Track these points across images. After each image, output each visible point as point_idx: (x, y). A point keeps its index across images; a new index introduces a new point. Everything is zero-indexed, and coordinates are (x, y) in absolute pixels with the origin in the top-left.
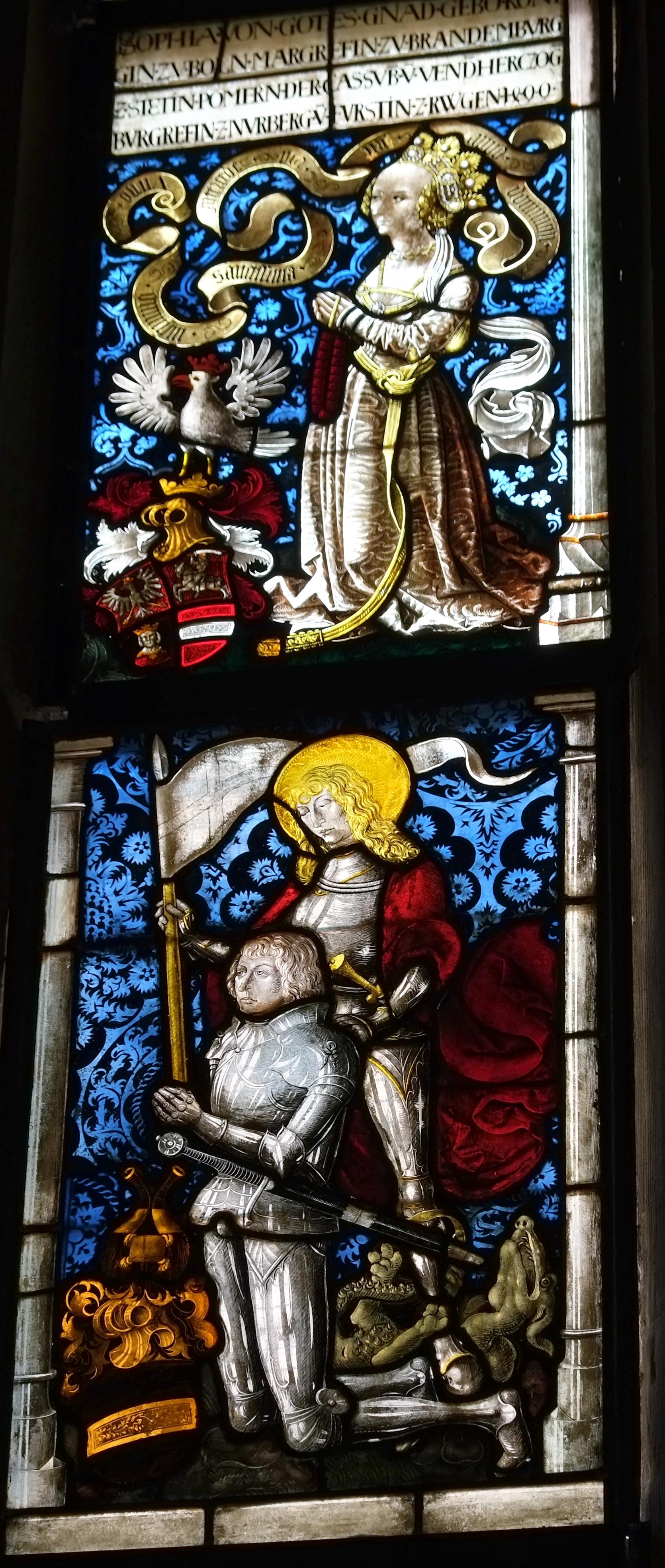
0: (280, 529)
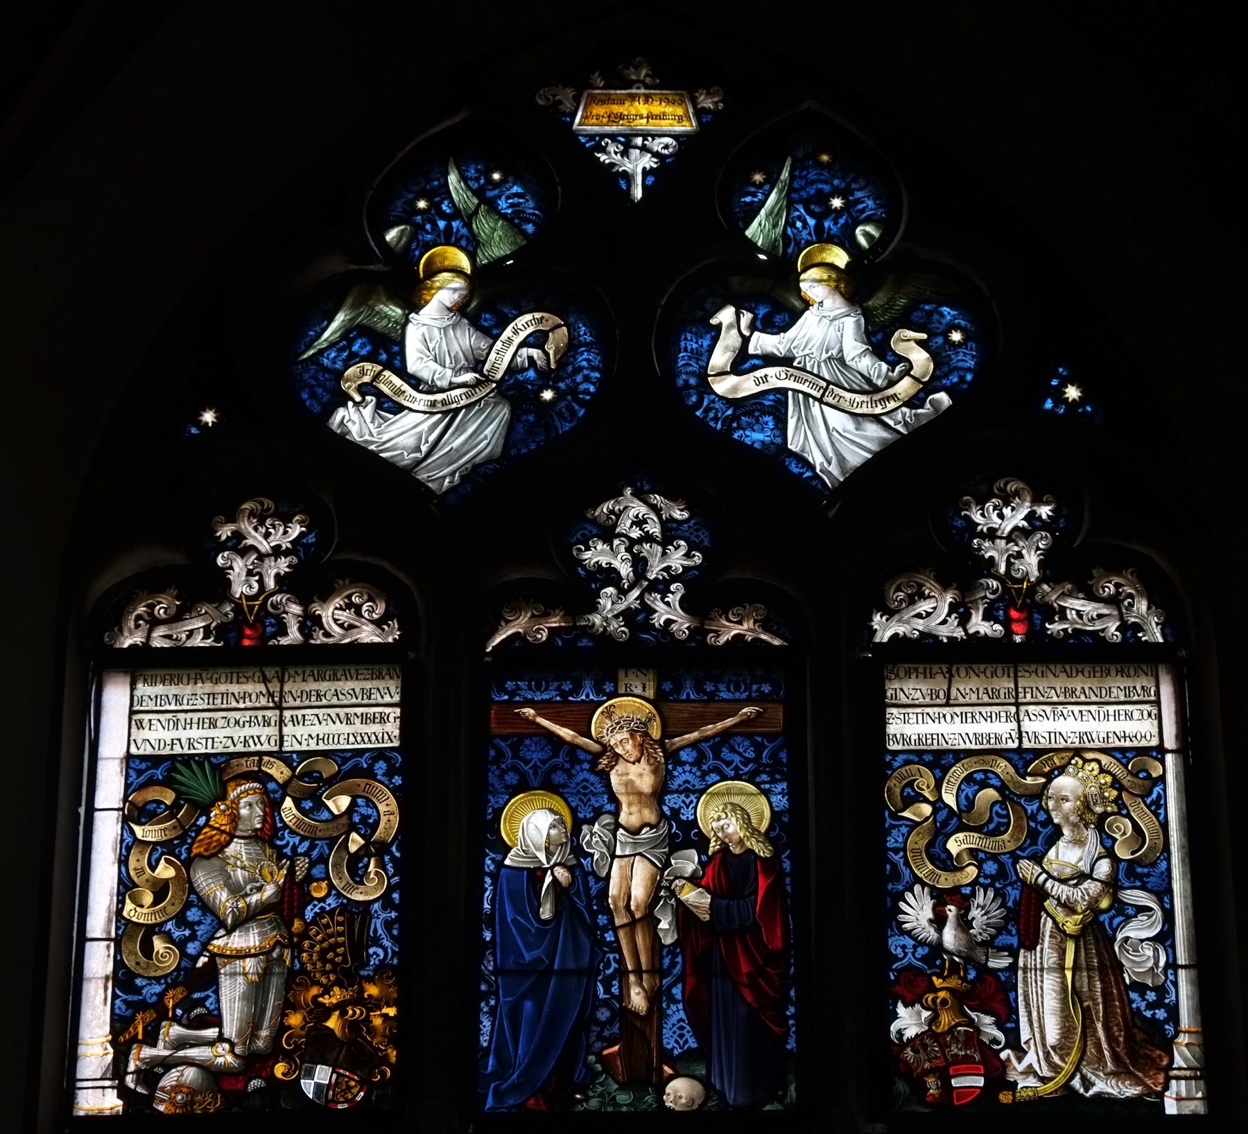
0: (1007, 1019)
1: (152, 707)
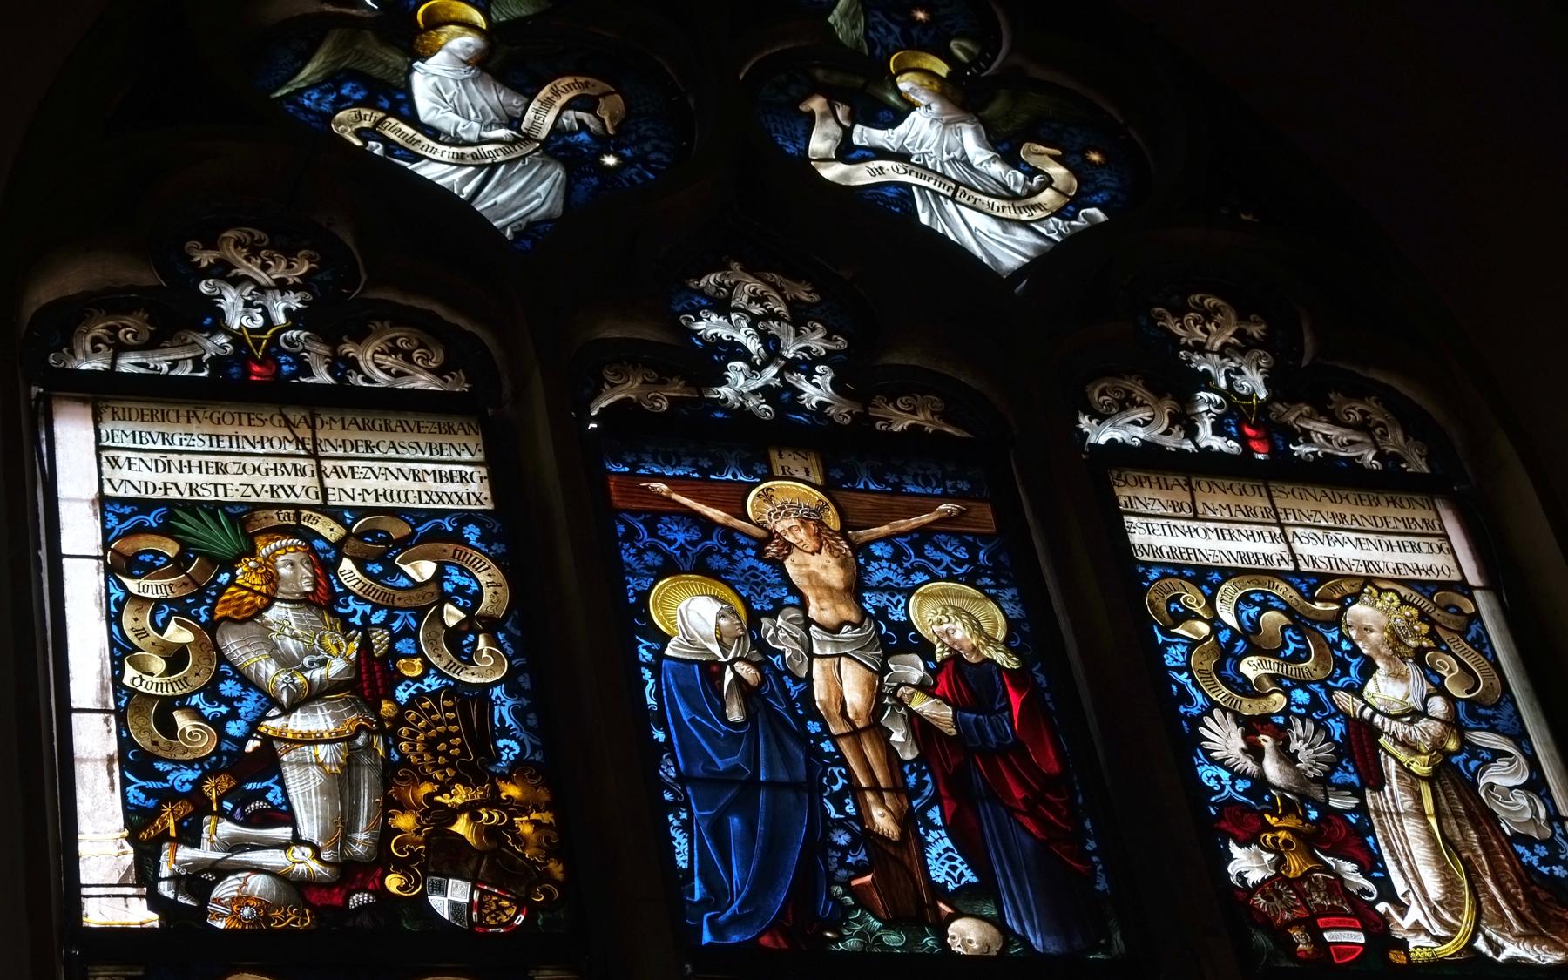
0: (1371, 864)
1: (128, 443)
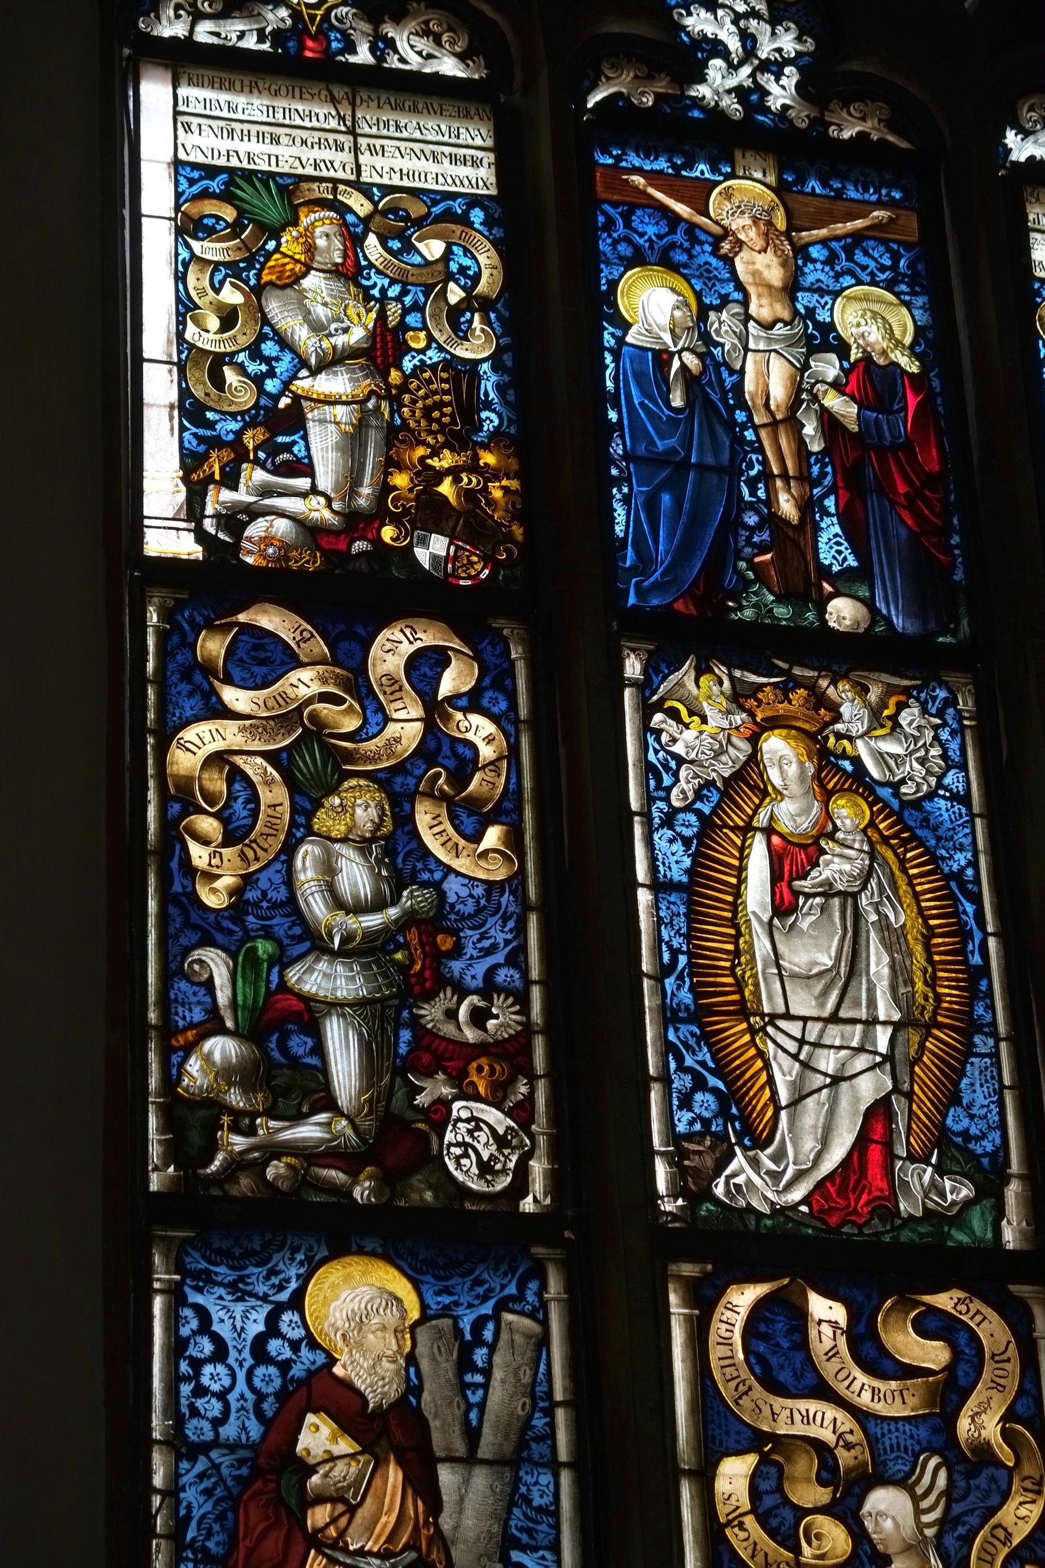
1: (200, 110)
